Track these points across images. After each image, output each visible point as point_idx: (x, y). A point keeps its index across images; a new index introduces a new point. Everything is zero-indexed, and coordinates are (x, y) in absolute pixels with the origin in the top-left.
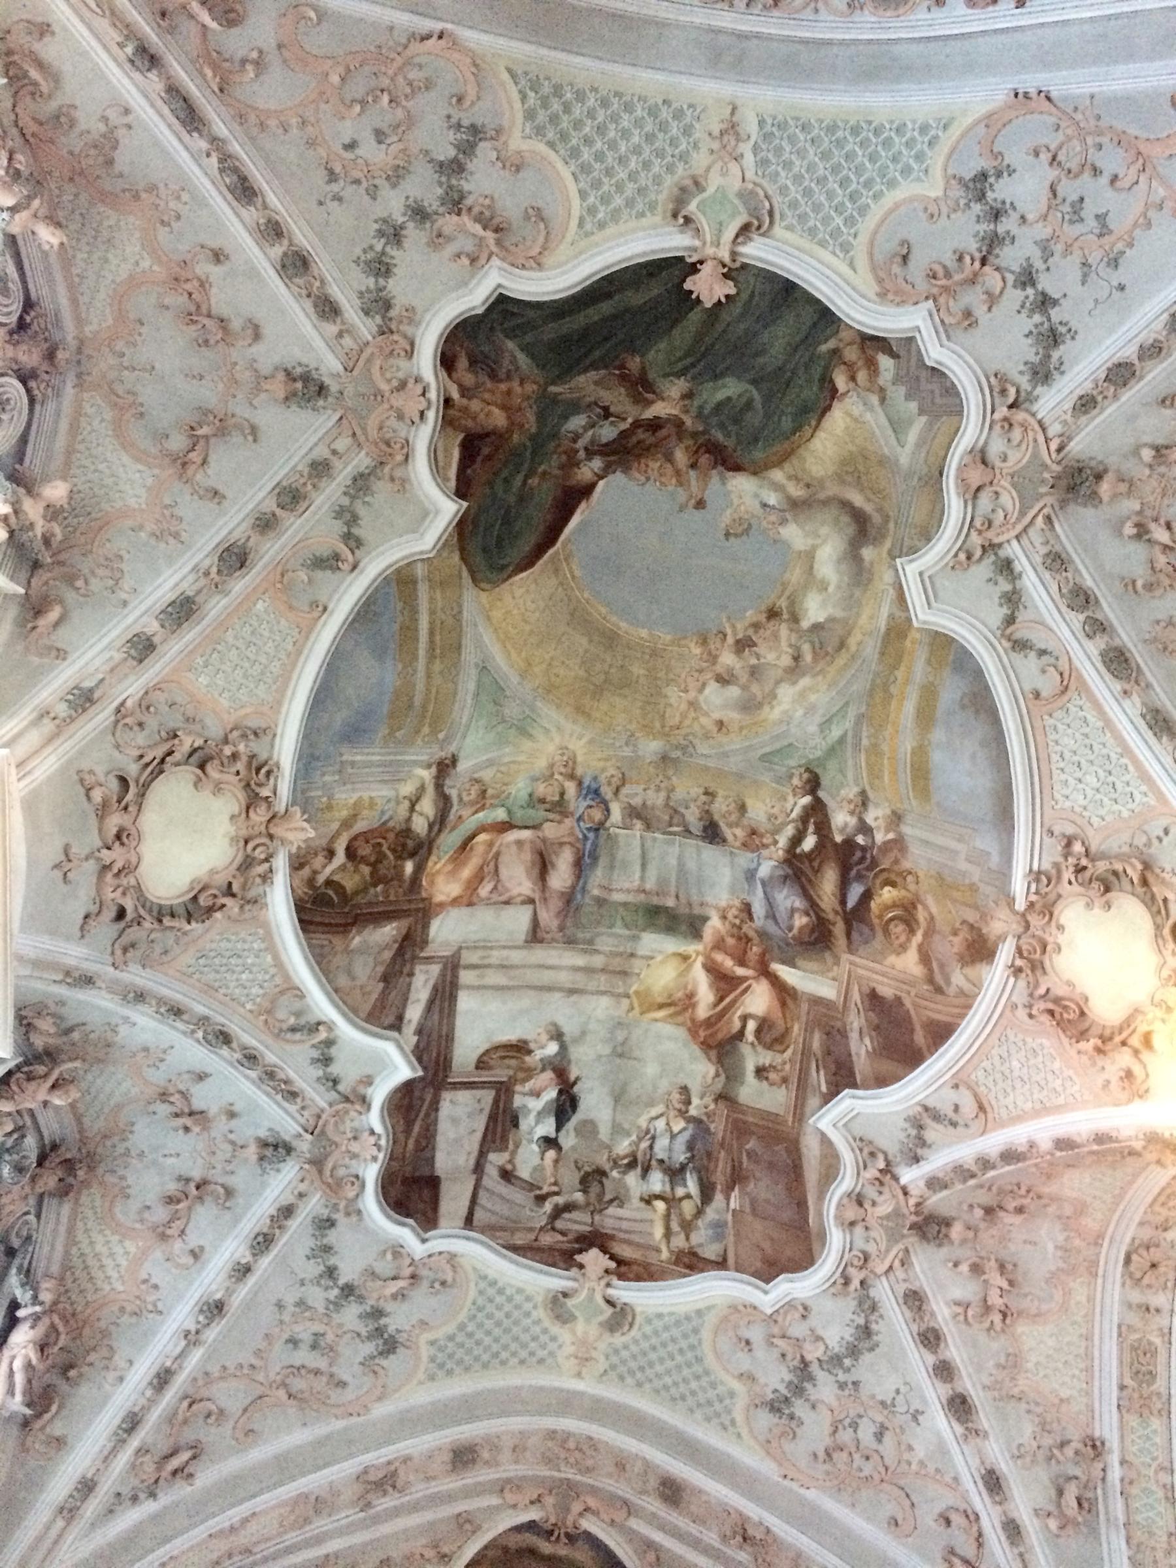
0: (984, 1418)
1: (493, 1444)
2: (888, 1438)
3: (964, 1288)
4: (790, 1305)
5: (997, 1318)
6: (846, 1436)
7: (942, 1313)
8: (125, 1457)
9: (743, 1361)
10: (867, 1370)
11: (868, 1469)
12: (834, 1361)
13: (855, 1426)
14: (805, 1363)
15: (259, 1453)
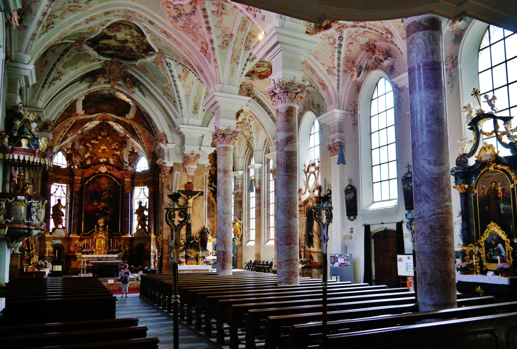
0: (213, 30)
1: (114, 11)
2: (195, 28)
3: (215, 9)
4: (179, 4)
5: (219, 14)
6: (187, 26)
7: (209, 12)
8: (40, 28)
9: (168, 9)
10: (192, 17)
11: (190, 31)
12: (187, 15)
13: (189, 25)
14: (181, 14)
15: (65, 21)
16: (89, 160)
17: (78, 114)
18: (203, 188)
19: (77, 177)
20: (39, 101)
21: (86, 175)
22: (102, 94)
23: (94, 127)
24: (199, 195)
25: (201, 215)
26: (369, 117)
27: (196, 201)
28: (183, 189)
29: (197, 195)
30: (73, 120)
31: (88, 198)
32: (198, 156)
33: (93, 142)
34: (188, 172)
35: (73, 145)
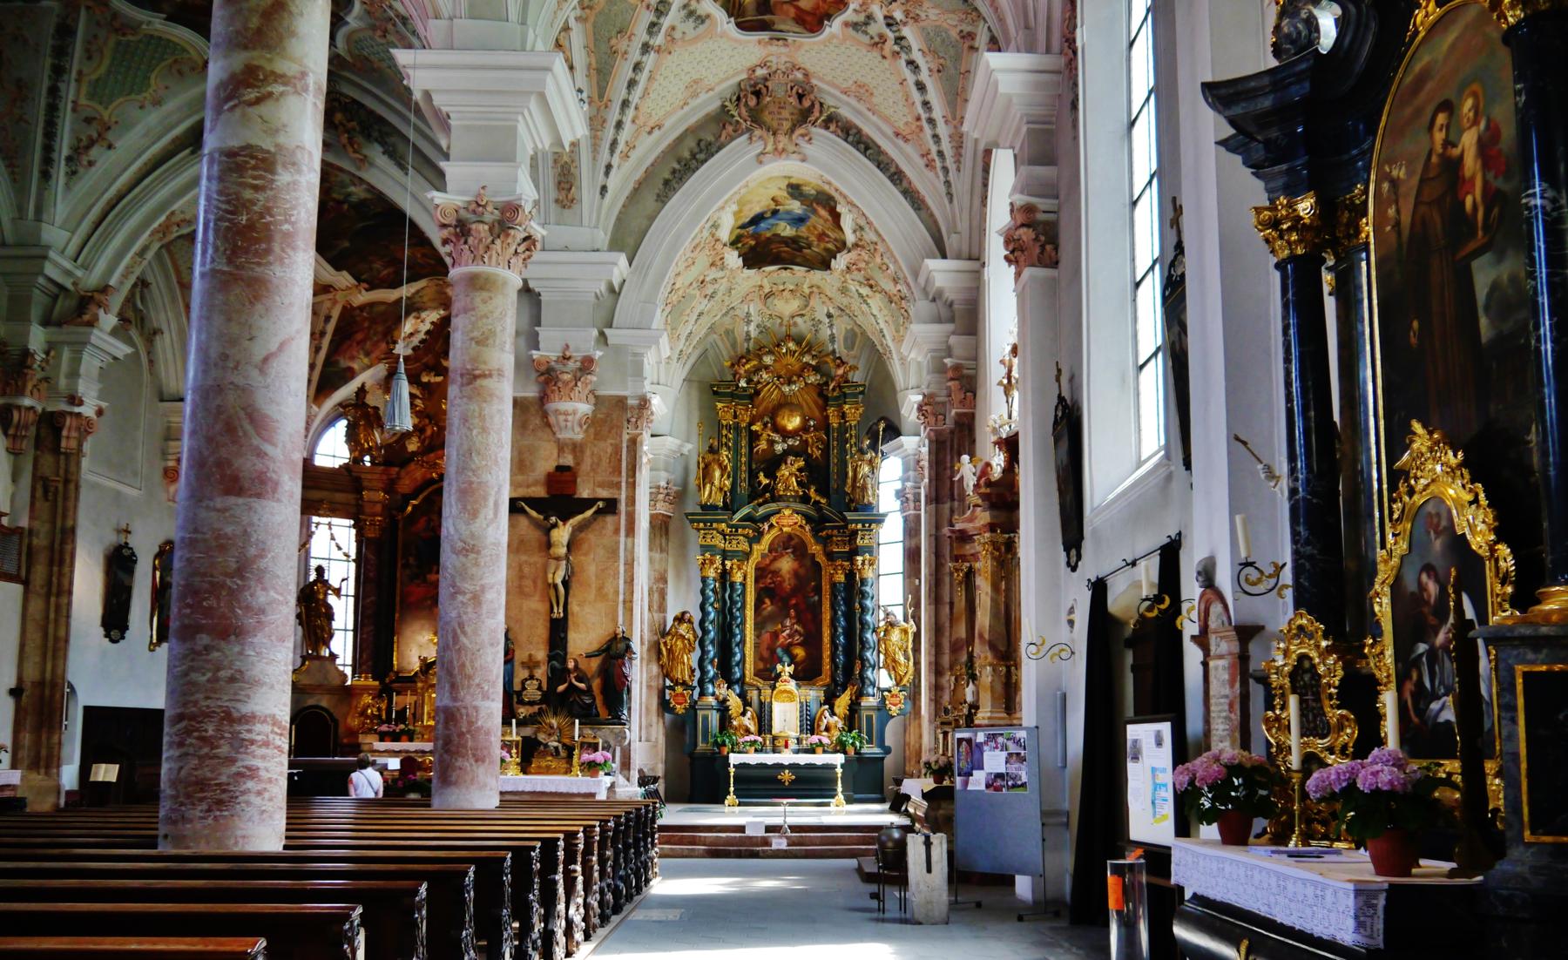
16: (415, 439)
17: (331, 286)
18: (618, 486)
19: (372, 493)
20: (44, 225)
21: (405, 485)
22: (354, 199)
23: (428, 332)
24: (599, 512)
25: (609, 589)
26: (1125, 44)
27: (591, 537)
28: (540, 492)
29: (589, 513)
30: (330, 310)
31: (411, 560)
32: (587, 365)
33: (425, 379)
34: (555, 429)
35: (362, 391)
